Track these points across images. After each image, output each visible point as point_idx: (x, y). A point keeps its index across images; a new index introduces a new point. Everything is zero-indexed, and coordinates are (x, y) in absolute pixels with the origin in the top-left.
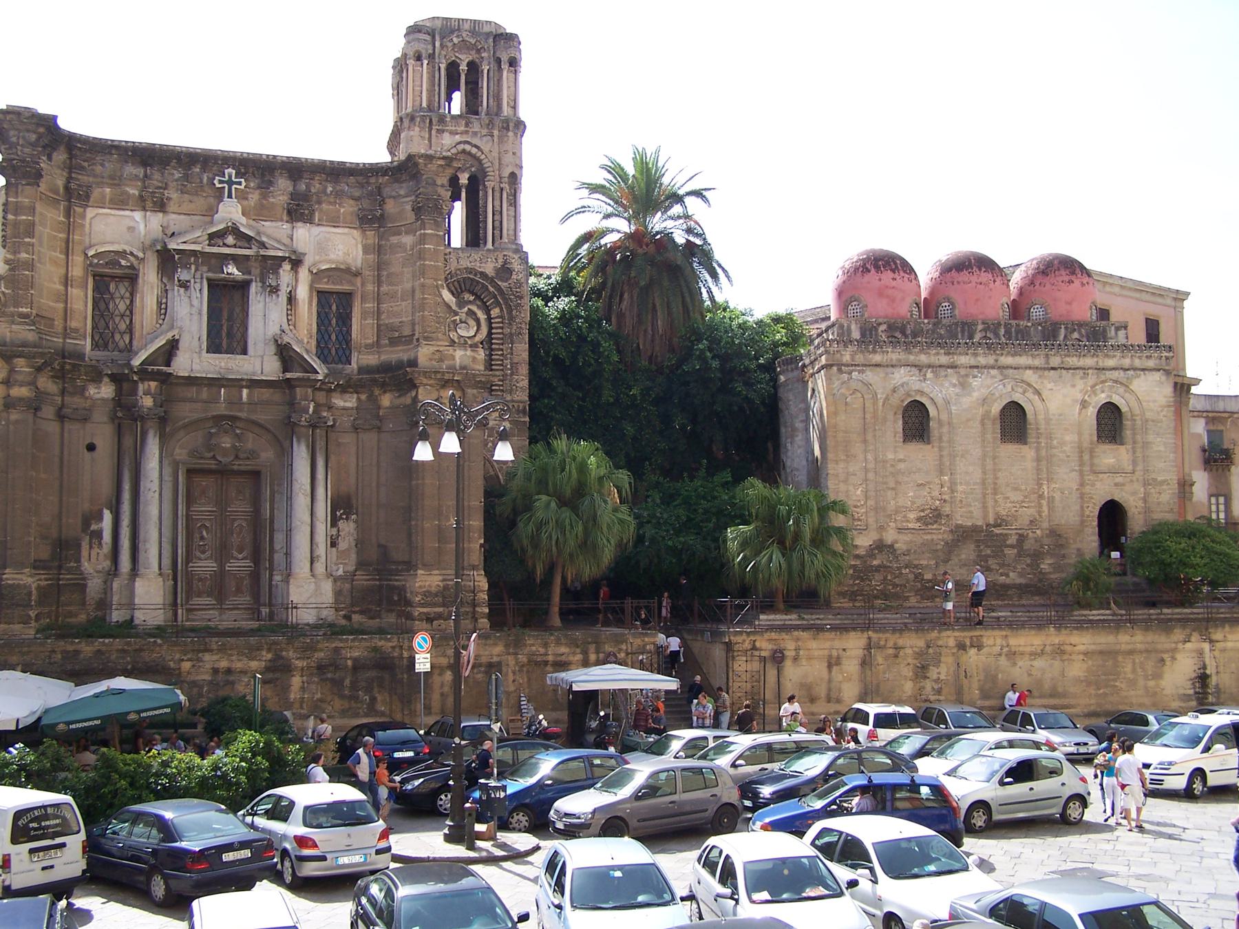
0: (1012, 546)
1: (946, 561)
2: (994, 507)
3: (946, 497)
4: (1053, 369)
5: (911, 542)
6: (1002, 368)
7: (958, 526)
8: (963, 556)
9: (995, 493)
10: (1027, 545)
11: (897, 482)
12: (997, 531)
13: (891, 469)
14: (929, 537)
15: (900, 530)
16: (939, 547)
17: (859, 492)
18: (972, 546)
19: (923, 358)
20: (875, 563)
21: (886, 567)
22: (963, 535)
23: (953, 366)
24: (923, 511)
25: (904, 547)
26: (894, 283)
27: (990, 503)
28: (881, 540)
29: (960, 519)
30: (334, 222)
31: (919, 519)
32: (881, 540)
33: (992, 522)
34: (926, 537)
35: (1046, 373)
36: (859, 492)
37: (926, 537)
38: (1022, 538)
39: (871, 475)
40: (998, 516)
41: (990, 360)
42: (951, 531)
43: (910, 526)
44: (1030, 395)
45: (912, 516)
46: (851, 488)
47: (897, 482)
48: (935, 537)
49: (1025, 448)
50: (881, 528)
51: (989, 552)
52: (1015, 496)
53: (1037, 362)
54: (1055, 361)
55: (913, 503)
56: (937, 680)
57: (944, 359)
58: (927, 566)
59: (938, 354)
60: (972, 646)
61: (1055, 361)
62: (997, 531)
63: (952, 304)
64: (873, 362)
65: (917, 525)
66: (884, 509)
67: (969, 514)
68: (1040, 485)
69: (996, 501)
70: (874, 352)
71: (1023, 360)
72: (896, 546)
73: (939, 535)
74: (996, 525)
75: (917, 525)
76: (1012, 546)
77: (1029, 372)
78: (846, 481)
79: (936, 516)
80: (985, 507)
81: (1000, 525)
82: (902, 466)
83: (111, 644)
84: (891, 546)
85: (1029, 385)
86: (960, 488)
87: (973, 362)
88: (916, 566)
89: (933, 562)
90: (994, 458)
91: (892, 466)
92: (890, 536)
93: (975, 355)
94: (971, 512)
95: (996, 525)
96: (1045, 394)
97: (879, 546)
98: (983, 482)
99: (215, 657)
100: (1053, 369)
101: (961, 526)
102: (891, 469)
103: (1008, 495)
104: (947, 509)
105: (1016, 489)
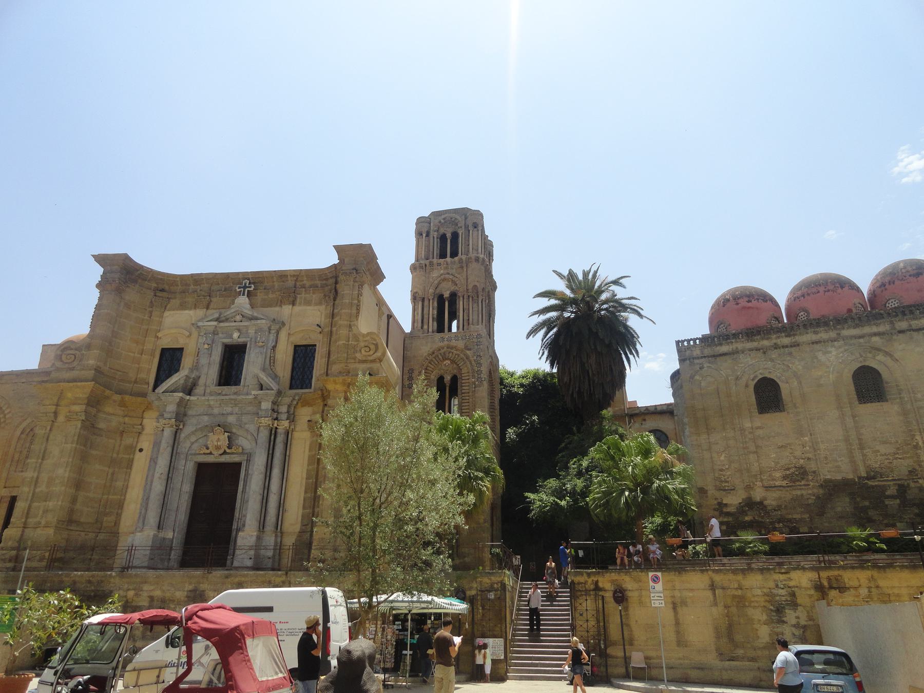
0: (892, 497)
1: (821, 514)
2: (864, 461)
3: (810, 456)
4: (901, 332)
5: (780, 498)
6: (845, 338)
7: (826, 481)
8: (839, 509)
9: (862, 447)
10: (910, 495)
11: (757, 447)
12: (870, 483)
13: (750, 436)
14: (799, 493)
15: (767, 488)
16: (810, 501)
17: (722, 458)
18: (847, 500)
19: (766, 343)
20: (746, 518)
21: (757, 522)
22: (834, 488)
23: (796, 345)
24: (788, 469)
25: (774, 503)
26: (750, 305)
27: (858, 457)
28: (750, 498)
29: (828, 473)
30: (308, 303)
31: (785, 478)
32: (750, 498)
33: (864, 474)
34: (794, 493)
35: (895, 337)
36: (722, 458)
37: (794, 493)
38: (903, 489)
39: (732, 442)
40: (869, 469)
41: (832, 334)
42: (821, 486)
43: (777, 483)
44: (880, 357)
45: (778, 475)
46: (715, 455)
47: (757, 447)
48: (804, 492)
49: (885, 406)
50: (748, 488)
51: (867, 503)
52: (883, 449)
53: (881, 329)
54: (903, 325)
55: (777, 463)
56: (796, 626)
57: (786, 341)
58: (801, 520)
59: (779, 337)
60: (831, 588)
61: (903, 325)
62: (870, 483)
63: (806, 311)
64: (721, 352)
65: (784, 483)
66: (748, 470)
67: (840, 468)
68: (914, 435)
69: (864, 455)
70: (721, 344)
71: (867, 330)
72: (766, 503)
73: (809, 491)
74: (868, 478)
75: (784, 483)
76: (892, 497)
77: (875, 339)
78: (710, 449)
79: (799, 475)
80: (853, 462)
81: (874, 478)
82: (760, 432)
83: (82, 576)
84: (761, 503)
85: (879, 350)
86: (822, 446)
87: (815, 337)
88: (790, 520)
89: (806, 516)
90: (854, 417)
91: (750, 433)
92: (758, 494)
93: (816, 333)
94: (838, 467)
95: (868, 478)
96: (897, 355)
97: (750, 504)
98: (847, 440)
99: (152, 588)
100: (901, 332)
101: (830, 481)
102: (750, 436)
103: (877, 448)
104: (812, 466)
105: (885, 443)
